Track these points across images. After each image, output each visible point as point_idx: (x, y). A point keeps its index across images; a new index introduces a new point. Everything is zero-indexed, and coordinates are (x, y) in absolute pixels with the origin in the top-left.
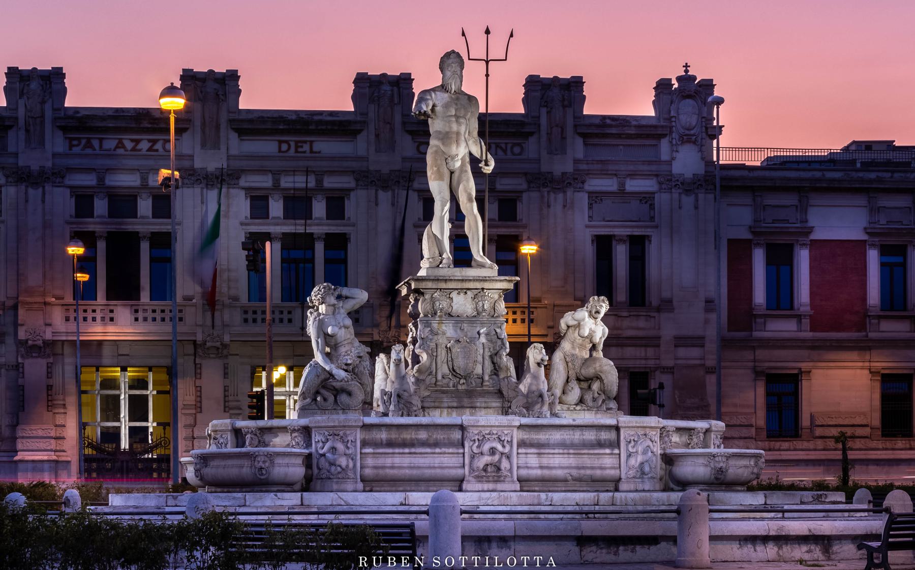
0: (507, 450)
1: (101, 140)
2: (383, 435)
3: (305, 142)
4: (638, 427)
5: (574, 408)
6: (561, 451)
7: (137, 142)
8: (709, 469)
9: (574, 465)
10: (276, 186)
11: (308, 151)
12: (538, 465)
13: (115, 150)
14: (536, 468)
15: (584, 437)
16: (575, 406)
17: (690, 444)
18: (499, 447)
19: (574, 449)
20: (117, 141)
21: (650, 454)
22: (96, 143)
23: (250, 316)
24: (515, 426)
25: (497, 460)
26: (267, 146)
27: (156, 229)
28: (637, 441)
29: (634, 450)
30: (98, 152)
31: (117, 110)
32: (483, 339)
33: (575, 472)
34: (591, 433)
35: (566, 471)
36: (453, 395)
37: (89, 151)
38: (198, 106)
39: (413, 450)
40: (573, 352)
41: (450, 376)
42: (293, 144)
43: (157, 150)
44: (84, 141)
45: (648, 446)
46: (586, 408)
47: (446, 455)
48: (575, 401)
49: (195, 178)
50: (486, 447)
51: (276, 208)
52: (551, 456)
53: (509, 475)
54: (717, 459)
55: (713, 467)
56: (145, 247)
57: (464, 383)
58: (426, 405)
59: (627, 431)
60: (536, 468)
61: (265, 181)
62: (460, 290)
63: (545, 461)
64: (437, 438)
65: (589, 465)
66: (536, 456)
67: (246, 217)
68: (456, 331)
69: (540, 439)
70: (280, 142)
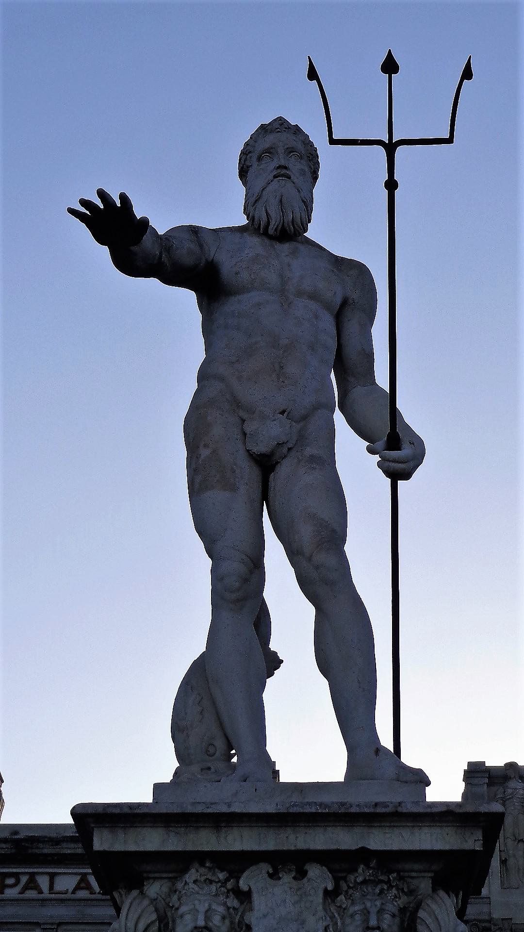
1: (52, 876)
13: (73, 892)
20: (79, 877)
22: (43, 882)
30: (46, 894)
37: (31, 894)
44: (24, 879)
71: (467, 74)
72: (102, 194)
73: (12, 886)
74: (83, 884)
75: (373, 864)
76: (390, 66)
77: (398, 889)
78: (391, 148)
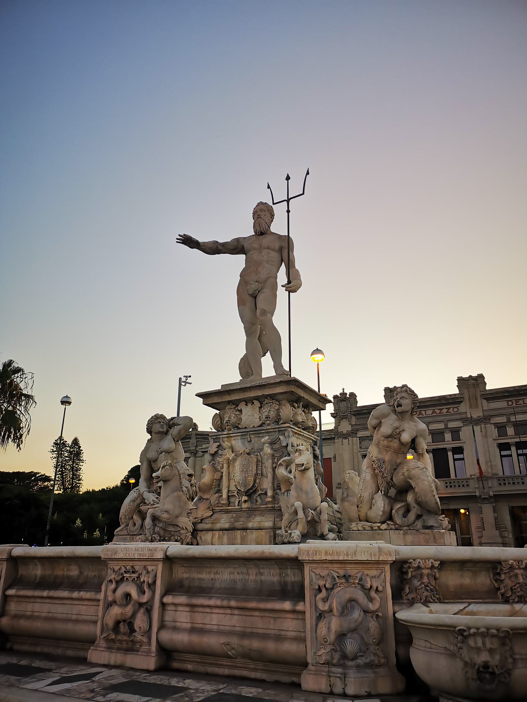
0: (144, 599)
2: (38, 571)
3: (520, 400)
4: (332, 562)
5: (379, 527)
6: (219, 603)
7: (441, 410)
8: (460, 665)
9: (238, 629)
10: (509, 421)
11: (522, 403)
12: (189, 626)
14: (184, 630)
15: (263, 578)
16: (379, 525)
17: (499, 589)
18: (134, 593)
19: (237, 600)
20: (432, 410)
21: (357, 614)
22: (423, 412)
23: (502, 482)
24: (158, 560)
25: (130, 614)
26: (501, 404)
27: (454, 446)
28: (332, 589)
29: (326, 608)
31: (431, 398)
32: (268, 450)
33: (235, 641)
34: (272, 571)
35: (223, 640)
36: (234, 515)
37: (420, 416)
38: (466, 392)
39: (52, 593)
40: (380, 456)
41: (235, 494)
42: (514, 401)
43: (450, 412)
44: (418, 412)
45: (352, 600)
46: (393, 527)
47: (86, 603)
48: (379, 519)
49: (469, 422)
50: (120, 592)
51: (510, 431)
52: (208, 610)
53: (145, 640)
54: (471, 642)
55: (467, 659)
56: (450, 454)
57: (245, 501)
58: (200, 526)
59: (316, 568)
60: (184, 630)
61: (503, 419)
62: (248, 401)
63: (200, 619)
64: (87, 576)
65: (261, 631)
66: (187, 609)
67: (496, 437)
68: (243, 443)
69: (203, 580)
70: (508, 401)
71: (308, 173)
72: (179, 235)
73: (416, 414)
74: (434, 412)
75: (268, 398)
76: (288, 178)
77: (275, 404)
78: (288, 201)
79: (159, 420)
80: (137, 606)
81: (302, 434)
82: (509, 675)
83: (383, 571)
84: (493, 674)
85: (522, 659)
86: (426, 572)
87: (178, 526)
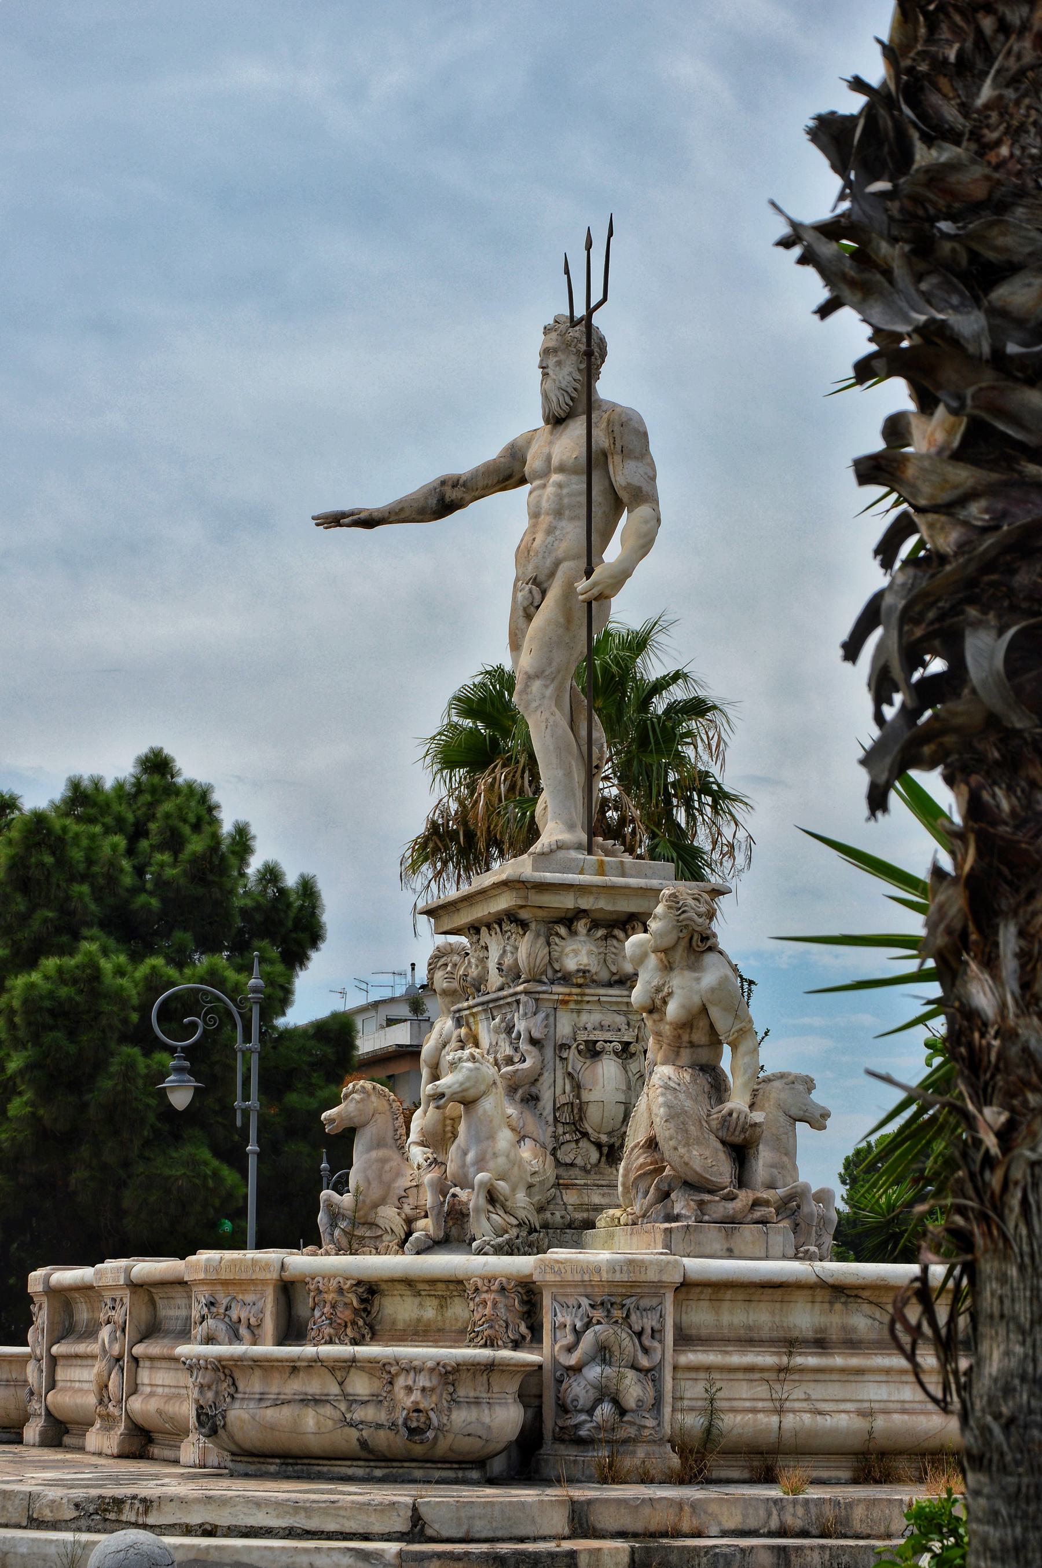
79: (442, 961)
80: (113, 1361)
81: (596, 998)
82: (224, 1417)
83: (263, 1295)
84: (207, 1414)
85: (243, 1399)
86: (330, 1297)
87: (377, 1226)
